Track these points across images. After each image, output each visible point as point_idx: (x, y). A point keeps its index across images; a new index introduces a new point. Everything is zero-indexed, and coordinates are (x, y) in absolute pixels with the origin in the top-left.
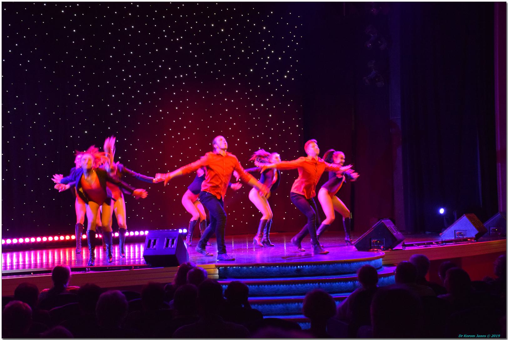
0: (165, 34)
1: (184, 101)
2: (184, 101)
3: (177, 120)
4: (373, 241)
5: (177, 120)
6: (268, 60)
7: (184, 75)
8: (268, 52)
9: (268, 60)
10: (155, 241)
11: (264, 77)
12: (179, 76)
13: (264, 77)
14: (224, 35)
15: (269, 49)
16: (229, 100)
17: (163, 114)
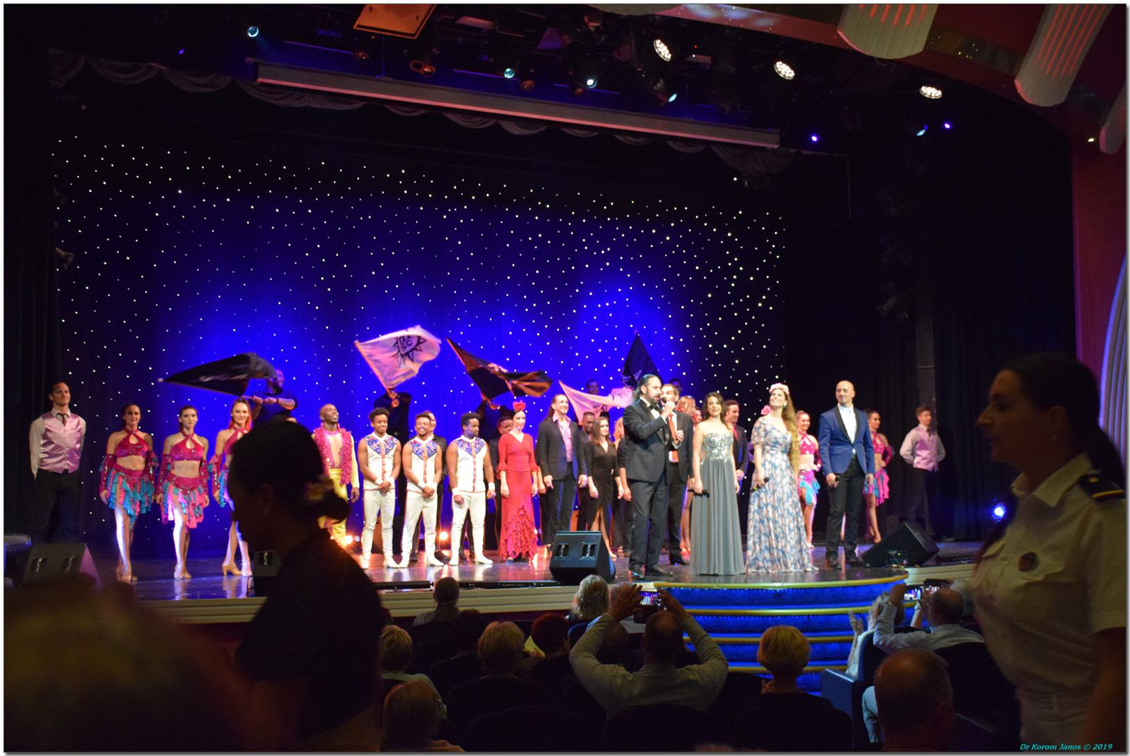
0: (585, 244)
1: (611, 339)
2: (611, 339)
3: (600, 367)
4: (893, 553)
5: (600, 367)
6: (734, 281)
7: (611, 303)
8: (735, 269)
9: (734, 281)
10: (567, 547)
11: (729, 305)
12: (603, 305)
13: (729, 305)
14: (670, 245)
15: (736, 265)
16: (676, 339)
17: (581, 359)
